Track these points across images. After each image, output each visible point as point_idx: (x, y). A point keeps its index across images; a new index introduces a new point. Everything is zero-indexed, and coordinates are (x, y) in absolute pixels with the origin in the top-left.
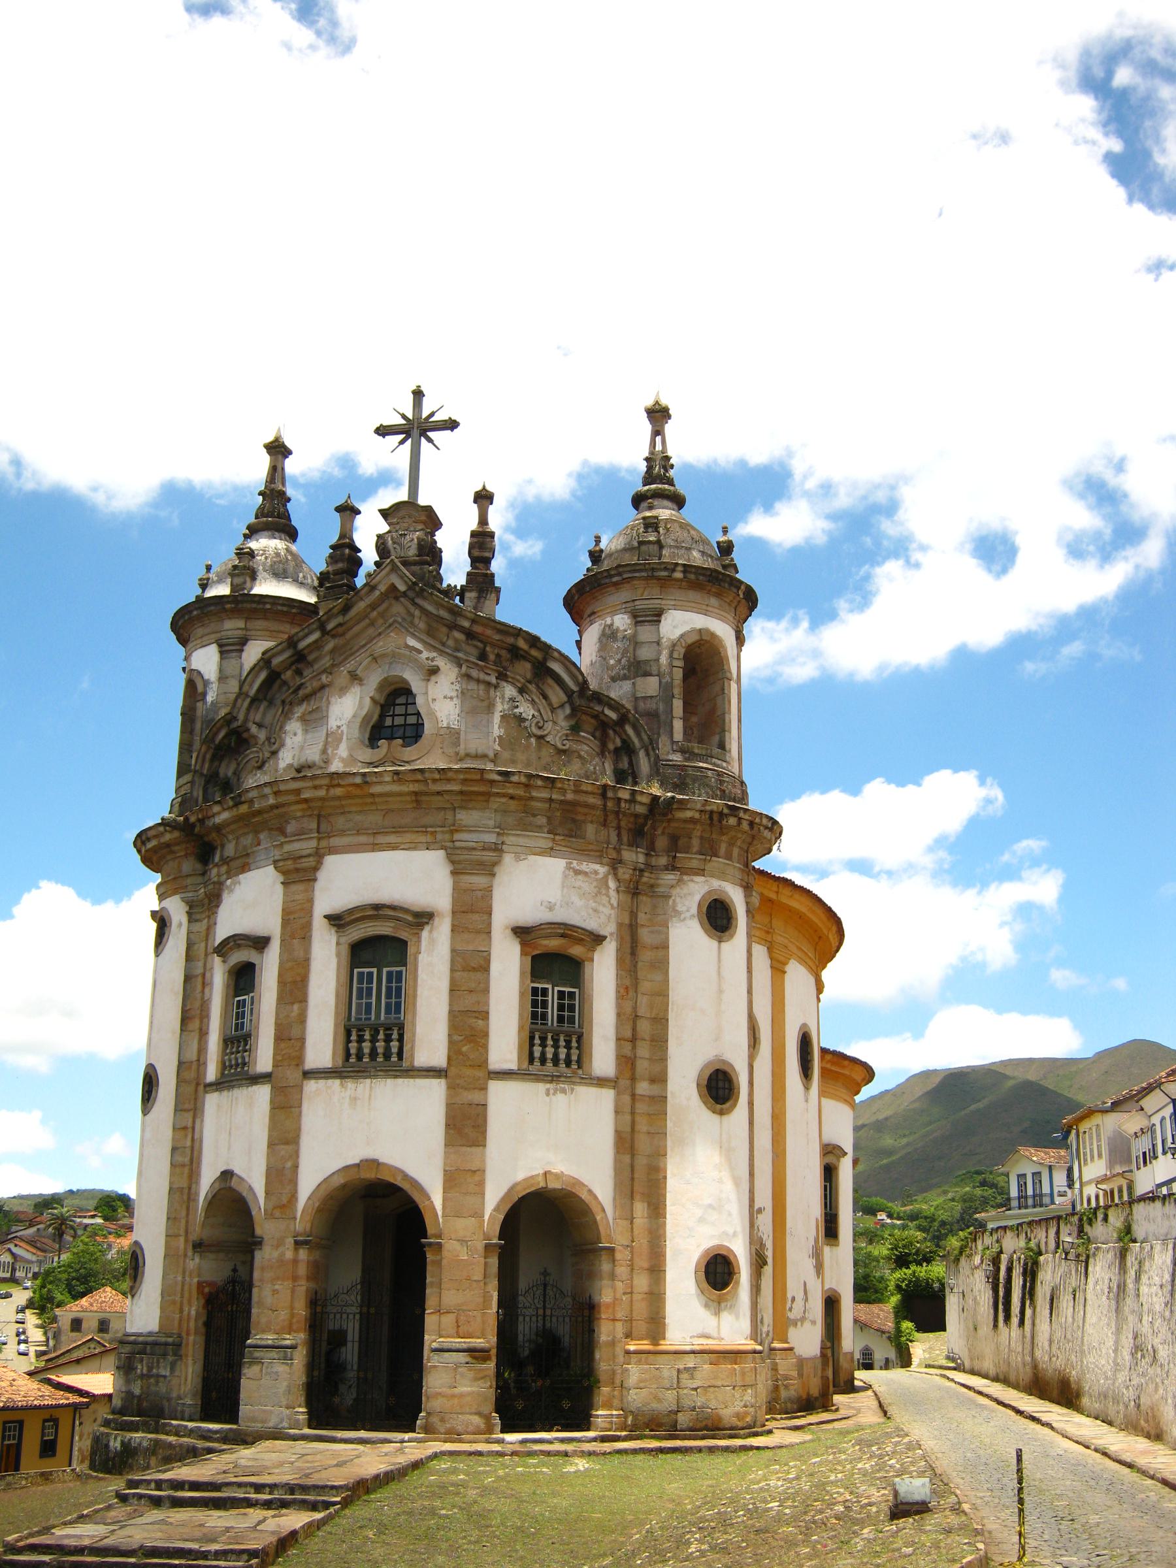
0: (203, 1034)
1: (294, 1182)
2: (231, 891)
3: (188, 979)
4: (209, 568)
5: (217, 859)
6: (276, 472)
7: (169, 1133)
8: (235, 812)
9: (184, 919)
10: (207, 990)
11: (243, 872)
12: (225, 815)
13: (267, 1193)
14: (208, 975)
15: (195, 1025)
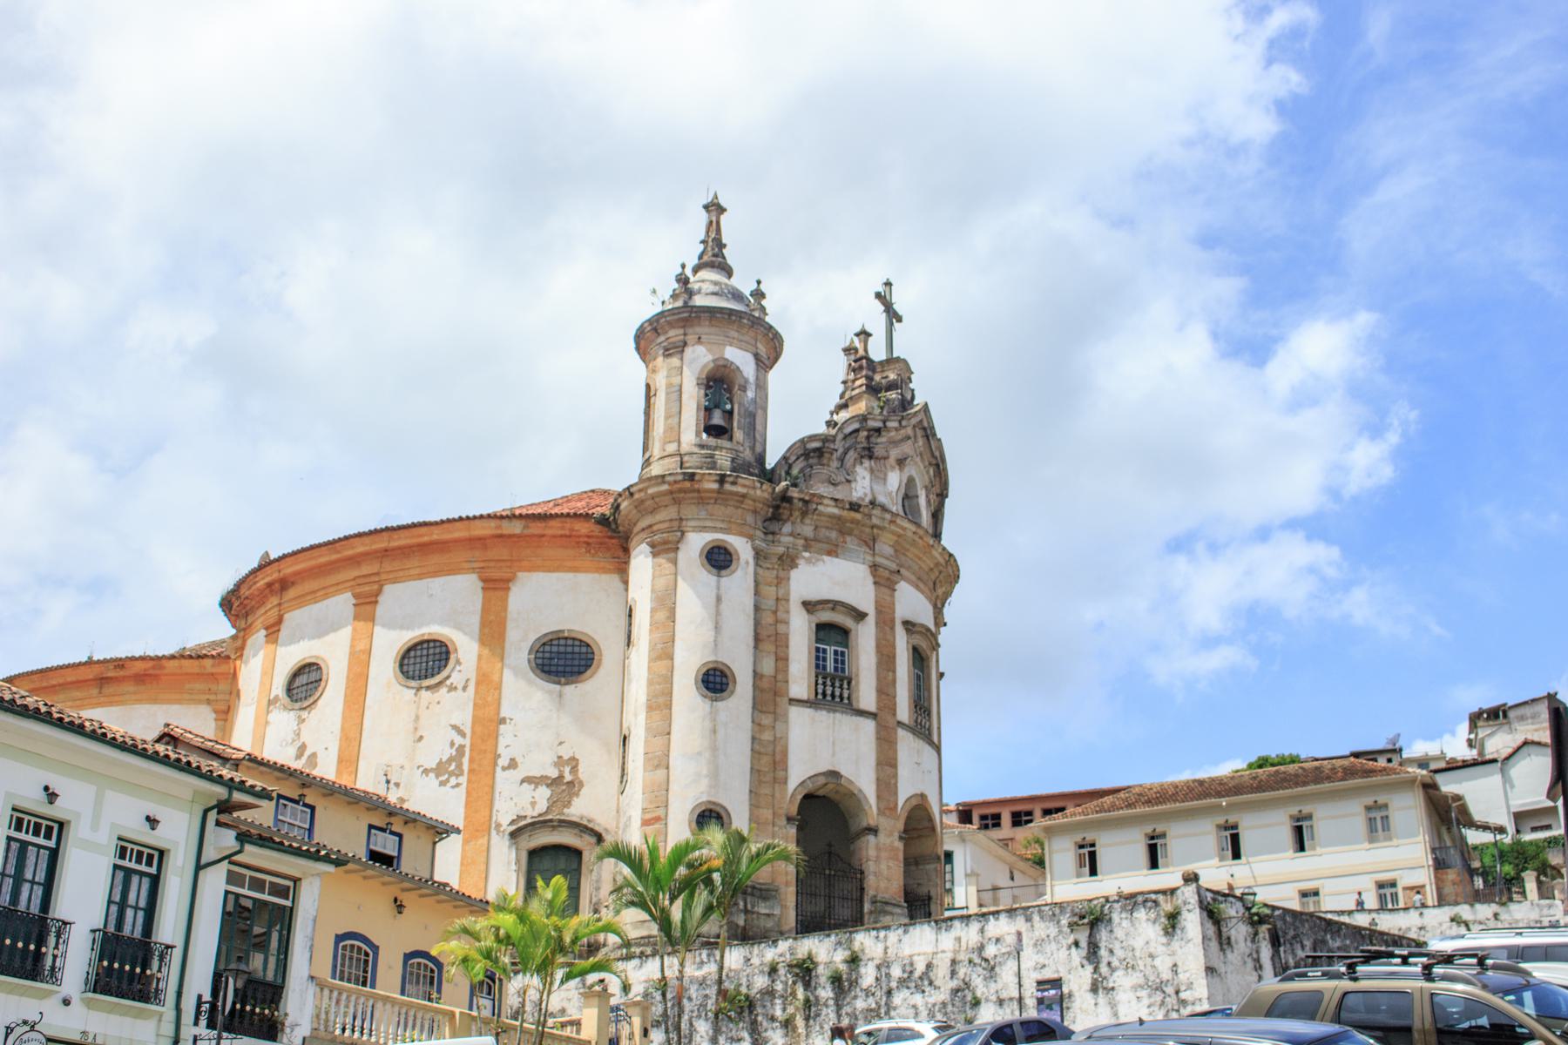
0: (782, 660)
1: (896, 794)
2: (809, 561)
3: (757, 608)
4: (683, 266)
5: (787, 528)
6: (714, 228)
7: (749, 724)
8: (845, 513)
9: (751, 561)
10: (781, 628)
11: (829, 553)
12: (836, 511)
13: (879, 797)
14: (780, 615)
15: (768, 647)
